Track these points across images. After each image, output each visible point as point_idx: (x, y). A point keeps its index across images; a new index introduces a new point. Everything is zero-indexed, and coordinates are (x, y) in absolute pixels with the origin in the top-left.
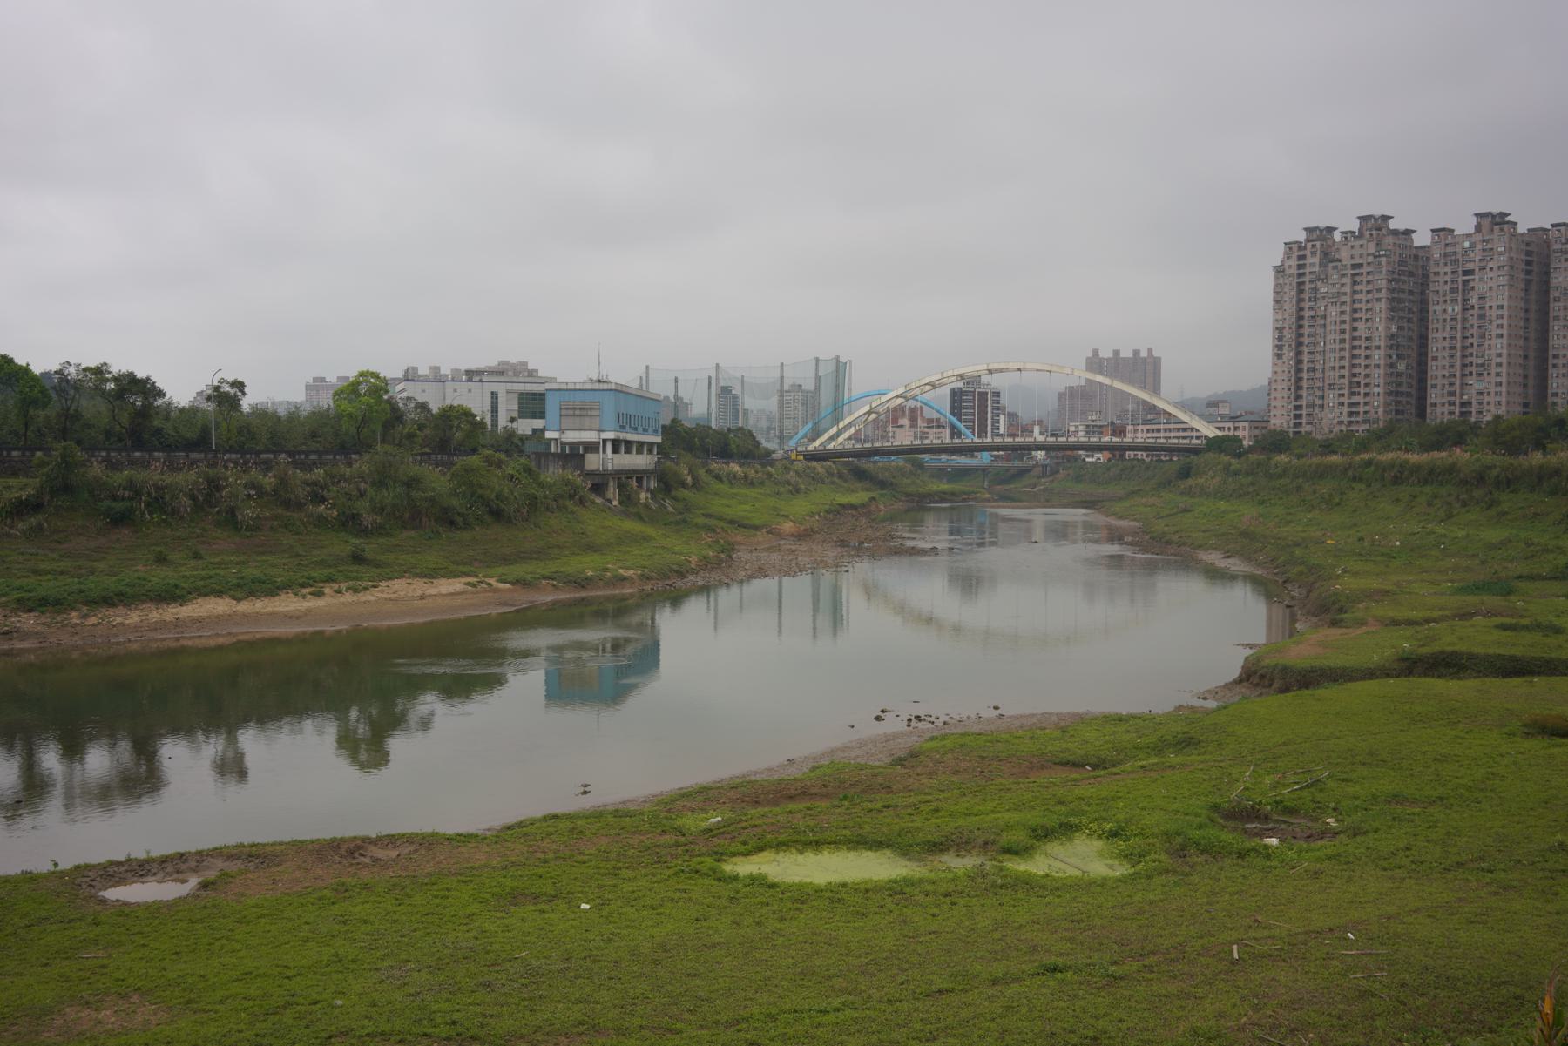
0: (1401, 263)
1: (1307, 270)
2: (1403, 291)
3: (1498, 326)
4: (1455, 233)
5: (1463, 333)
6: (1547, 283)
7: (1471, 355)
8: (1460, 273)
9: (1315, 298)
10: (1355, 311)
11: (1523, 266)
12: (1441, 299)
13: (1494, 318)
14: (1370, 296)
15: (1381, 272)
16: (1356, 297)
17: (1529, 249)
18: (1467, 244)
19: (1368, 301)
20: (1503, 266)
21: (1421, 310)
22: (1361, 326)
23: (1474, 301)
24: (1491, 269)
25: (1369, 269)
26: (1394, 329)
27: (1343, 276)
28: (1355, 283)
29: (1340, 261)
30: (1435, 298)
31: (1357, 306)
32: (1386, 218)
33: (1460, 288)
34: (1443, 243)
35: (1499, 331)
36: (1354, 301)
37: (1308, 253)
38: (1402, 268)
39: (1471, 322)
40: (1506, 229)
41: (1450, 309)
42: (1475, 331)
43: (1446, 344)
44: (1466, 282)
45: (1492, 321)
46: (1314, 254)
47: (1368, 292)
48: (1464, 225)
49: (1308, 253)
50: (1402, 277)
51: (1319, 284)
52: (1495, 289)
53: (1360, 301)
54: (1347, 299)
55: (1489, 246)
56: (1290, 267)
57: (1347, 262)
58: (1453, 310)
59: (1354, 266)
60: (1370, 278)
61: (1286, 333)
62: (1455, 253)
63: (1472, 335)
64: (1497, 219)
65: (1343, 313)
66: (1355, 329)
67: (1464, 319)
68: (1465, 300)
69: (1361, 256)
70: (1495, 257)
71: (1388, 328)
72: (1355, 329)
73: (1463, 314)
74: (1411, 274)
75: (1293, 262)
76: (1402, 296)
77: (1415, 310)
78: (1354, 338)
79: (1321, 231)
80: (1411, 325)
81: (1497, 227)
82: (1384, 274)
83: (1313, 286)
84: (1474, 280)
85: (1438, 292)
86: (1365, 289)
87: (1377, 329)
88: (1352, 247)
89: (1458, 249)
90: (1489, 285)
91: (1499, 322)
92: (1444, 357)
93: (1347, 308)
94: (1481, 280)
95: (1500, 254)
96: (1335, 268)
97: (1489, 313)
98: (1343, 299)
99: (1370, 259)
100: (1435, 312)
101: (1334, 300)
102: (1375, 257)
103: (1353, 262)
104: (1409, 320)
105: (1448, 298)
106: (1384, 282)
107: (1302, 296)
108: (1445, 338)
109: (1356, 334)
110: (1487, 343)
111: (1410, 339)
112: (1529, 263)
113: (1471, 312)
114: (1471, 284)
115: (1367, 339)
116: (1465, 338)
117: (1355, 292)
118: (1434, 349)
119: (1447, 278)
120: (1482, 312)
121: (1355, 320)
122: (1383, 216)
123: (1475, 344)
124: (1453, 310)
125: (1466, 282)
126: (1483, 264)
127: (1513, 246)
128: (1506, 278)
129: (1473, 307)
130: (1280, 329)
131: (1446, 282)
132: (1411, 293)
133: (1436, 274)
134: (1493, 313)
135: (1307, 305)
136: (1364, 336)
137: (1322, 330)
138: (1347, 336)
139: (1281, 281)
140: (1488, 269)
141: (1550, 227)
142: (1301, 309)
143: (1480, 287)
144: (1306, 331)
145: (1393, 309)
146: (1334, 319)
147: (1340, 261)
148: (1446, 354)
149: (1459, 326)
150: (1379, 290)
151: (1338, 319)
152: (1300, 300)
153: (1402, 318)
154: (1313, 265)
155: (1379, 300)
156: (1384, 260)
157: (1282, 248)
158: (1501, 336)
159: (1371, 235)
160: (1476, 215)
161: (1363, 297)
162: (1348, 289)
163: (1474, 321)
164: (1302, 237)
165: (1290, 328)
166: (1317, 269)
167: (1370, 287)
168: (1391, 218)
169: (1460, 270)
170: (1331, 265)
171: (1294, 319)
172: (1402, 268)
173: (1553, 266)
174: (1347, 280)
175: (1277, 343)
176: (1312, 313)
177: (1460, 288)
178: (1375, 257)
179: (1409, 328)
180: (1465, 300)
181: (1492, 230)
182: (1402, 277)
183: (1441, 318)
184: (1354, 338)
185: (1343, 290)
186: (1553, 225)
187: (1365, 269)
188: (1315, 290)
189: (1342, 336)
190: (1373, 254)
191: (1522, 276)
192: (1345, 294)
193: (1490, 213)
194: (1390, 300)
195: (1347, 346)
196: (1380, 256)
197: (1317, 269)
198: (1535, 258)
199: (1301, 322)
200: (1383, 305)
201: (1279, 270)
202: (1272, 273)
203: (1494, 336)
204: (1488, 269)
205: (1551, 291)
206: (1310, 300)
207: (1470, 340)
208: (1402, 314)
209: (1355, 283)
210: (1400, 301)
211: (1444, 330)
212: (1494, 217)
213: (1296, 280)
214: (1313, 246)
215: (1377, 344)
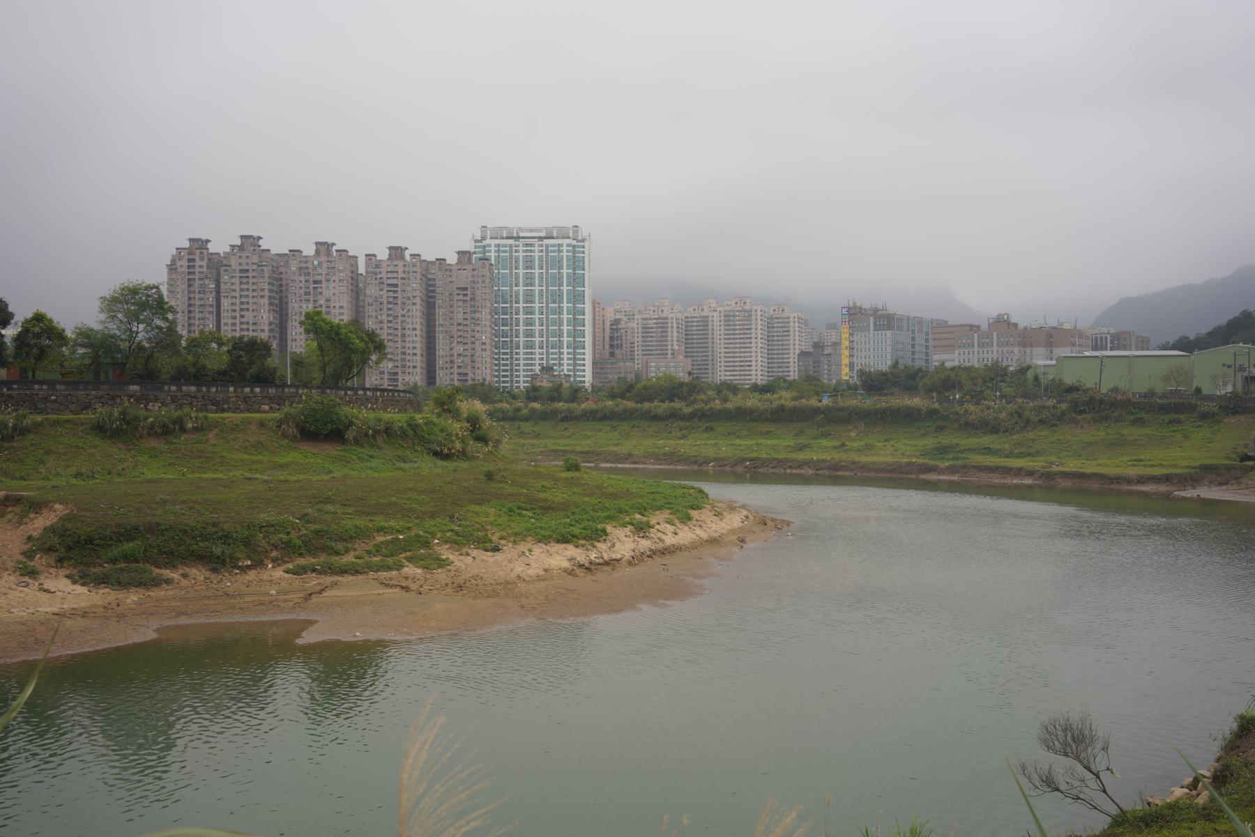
1: (197, 270)
8: (312, 282)
14: (255, 294)
15: (263, 277)
16: (243, 293)
18: (316, 263)
19: (253, 297)
20: (343, 280)
21: (281, 303)
24: (334, 281)
26: (272, 319)
27: (232, 277)
33: (312, 292)
41: (304, 306)
47: (254, 290)
51: (207, 281)
53: (247, 296)
54: (237, 295)
56: (182, 266)
58: (307, 307)
59: (241, 271)
60: (255, 280)
62: (307, 268)
65: (233, 304)
68: (315, 301)
70: (337, 273)
71: (269, 318)
72: (242, 316)
75: (184, 263)
76: (275, 295)
82: (266, 279)
83: (202, 282)
84: (321, 287)
85: (295, 294)
86: (251, 289)
87: (262, 317)
88: (240, 257)
89: (310, 266)
92: (301, 340)
94: (327, 288)
95: (341, 271)
96: (226, 271)
97: (333, 311)
98: (234, 294)
99: (255, 267)
100: (294, 307)
102: (258, 266)
106: (266, 284)
107: (191, 289)
109: (243, 320)
114: (320, 290)
115: (254, 324)
120: (328, 310)
121: (242, 310)
124: (307, 307)
128: (345, 288)
129: (321, 306)
131: (301, 288)
137: (211, 316)
138: (237, 321)
143: (328, 293)
145: (271, 304)
147: (230, 266)
150: (263, 290)
154: (201, 267)
155: (262, 297)
156: (265, 268)
157: (174, 252)
164: (187, 245)
165: (183, 312)
166: (205, 270)
167: (255, 287)
169: (311, 280)
170: (222, 268)
174: (237, 281)
176: (202, 302)
177: (312, 292)
184: (242, 323)
185: (233, 287)
187: (250, 274)
188: (203, 286)
189: (233, 321)
190: (256, 264)
192: (234, 290)
194: (270, 297)
195: (238, 328)
196: (262, 266)
197: (205, 270)
199: (191, 309)
200: (266, 301)
202: (165, 270)
206: (199, 292)
209: (241, 283)
210: (275, 298)
213: (187, 277)
214: (201, 253)
215: (262, 328)
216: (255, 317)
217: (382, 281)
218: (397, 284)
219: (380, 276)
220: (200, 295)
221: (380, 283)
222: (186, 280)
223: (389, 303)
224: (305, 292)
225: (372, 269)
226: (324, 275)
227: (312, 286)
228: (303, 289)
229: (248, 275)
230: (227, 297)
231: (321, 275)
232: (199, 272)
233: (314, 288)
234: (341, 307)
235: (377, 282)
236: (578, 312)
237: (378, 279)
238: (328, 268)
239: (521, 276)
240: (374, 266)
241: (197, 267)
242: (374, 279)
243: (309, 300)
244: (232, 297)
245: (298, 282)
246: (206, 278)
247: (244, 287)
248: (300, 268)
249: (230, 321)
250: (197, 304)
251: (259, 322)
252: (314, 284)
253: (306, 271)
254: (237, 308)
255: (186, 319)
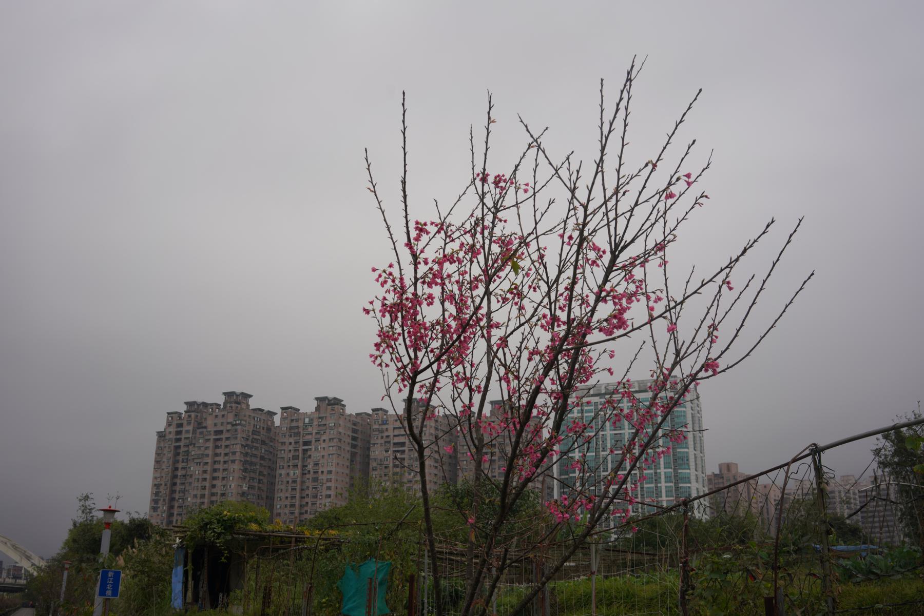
0: (254, 432)
1: (183, 436)
2: (255, 456)
3: (327, 487)
4: (300, 411)
5: (301, 493)
6: (368, 456)
7: (306, 512)
8: (301, 443)
9: (187, 459)
10: (215, 470)
11: (349, 440)
12: (286, 465)
13: (325, 481)
14: (226, 458)
15: (236, 438)
17: (355, 427)
18: (307, 420)
20: (333, 439)
22: (218, 483)
23: (310, 467)
24: (324, 441)
25: (228, 435)
26: (245, 488)
28: (217, 447)
29: (205, 427)
30: (281, 464)
31: (216, 466)
32: (247, 396)
33: (301, 456)
34: (289, 418)
35: (328, 492)
36: (215, 462)
37: (185, 422)
38: (255, 437)
39: (307, 484)
40: (336, 409)
41: (291, 473)
42: (309, 492)
43: (288, 502)
44: (305, 451)
45: (323, 484)
46: (189, 423)
47: (226, 454)
48: (308, 406)
49: (185, 422)
50: (255, 444)
52: (326, 457)
53: (219, 462)
54: (209, 460)
55: (323, 423)
56: (170, 433)
57: (211, 429)
58: (294, 474)
60: (228, 443)
61: (162, 489)
62: (298, 427)
63: (308, 495)
64: (332, 402)
65: (205, 472)
66: (214, 486)
67: (303, 482)
69: (222, 424)
70: (328, 431)
72: (214, 486)
73: (302, 478)
74: (263, 442)
75: (173, 429)
76: (254, 460)
77: (265, 473)
78: (213, 494)
79: (199, 405)
80: (261, 485)
81: (330, 407)
83: (186, 449)
84: (311, 449)
85: (283, 458)
86: (223, 452)
87: (230, 486)
88: (216, 416)
89: (301, 424)
90: (322, 454)
91: (329, 484)
93: (209, 468)
94: (316, 449)
95: (331, 428)
96: (201, 433)
99: (229, 427)
100: (281, 475)
101: (198, 461)
102: (233, 425)
103: (216, 429)
104: (260, 481)
105: (291, 464)
106: (239, 446)
108: (287, 498)
109: (214, 491)
110: (318, 502)
111: (259, 497)
112: (354, 439)
113: (307, 476)
114: (309, 453)
116: (303, 498)
117: (216, 455)
118: (278, 506)
119: (291, 448)
120: (316, 476)
121: (214, 478)
122: (243, 394)
123: (310, 503)
124: (294, 474)
125: (305, 451)
126: (318, 436)
127: (341, 423)
128: (334, 448)
130: (157, 486)
131: (290, 451)
132: (262, 458)
133: (283, 443)
134: (323, 477)
135: (180, 465)
136: (219, 492)
138: (207, 492)
139: (162, 445)
140: (322, 441)
141: (370, 412)
142: (177, 469)
143: (315, 455)
144: (178, 488)
145: (245, 470)
146: (197, 477)
147: (205, 427)
148: (287, 511)
149: (298, 488)
150: (234, 453)
151: (200, 477)
152: (176, 462)
153: (253, 479)
154: (187, 432)
155: (233, 461)
156: (239, 427)
158: (329, 496)
159: (231, 407)
160: (317, 399)
161: (221, 459)
162: (210, 452)
163: (309, 484)
164: (182, 409)
165: (166, 485)
166: (190, 435)
167: (227, 451)
168: (250, 396)
169: (301, 441)
170: (199, 431)
171: (169, 478)
172: (255, 437)
173: (372, 442)
174: (210, 444)
175: (154, 498)
176: (183, 472)
177: (301, 456)
178: (233, 425)
179: (259, 489)
180: (304, 466)
181: (326, 410)
182: (255, 444)
183: (285, 480)
184: (213, 494)
185: (207, 452)
186: (373, 410)
187: (224, 436)
188: (187, 452)
189: (203, 492)
191: (348, 448)
192: (207, 456)
193: (326, 398)
196: (236, 425)
198: (359, 436)
199: (175, 480)
200: (237, 466)
201: (161, 435)
202: (155, 438)
203: (324, 497)
204: (322, 441)
205: (371, 461)
207: (306, 500)
208: (252, 475)
209: (217, 447)
210: (252, 463)
211: (287, 490)
212: (329, 400)
214: (190, 416)
216: (224, 486)
217: (388, 440)
218: (405, 443)
219: (386, 434)
220: (184, 464)
221: (385, 442)
222: (172, 448)
223: (395, 466)
224: (293, 456)
225: (377, 427)
226: (314, 434)
227: (302, 448)
228: (292, 451)
229: (221, 436)
230: (200, 463)
231: (312, 434)
232: (186, 438)
233: (304, 450)
234: (330, 472)
235: (383, 441)
236: (682, 479)
237: (384, 437)
238: (319, 425)
239: (608, 439)
240: (380, 422)
241: (184, 432)
242: (380, 437)
243: (297, 465)
244: (207, 463)
245: (287, 444)
246: (191, 444)
247: (218, 451)
248: (291, 428)
249: (199, 493)
250: (179, 474)
251: (227, 492)
252: (304, 445)
253: (296, 431)
254: (208, 476)
255: (168, 493)
